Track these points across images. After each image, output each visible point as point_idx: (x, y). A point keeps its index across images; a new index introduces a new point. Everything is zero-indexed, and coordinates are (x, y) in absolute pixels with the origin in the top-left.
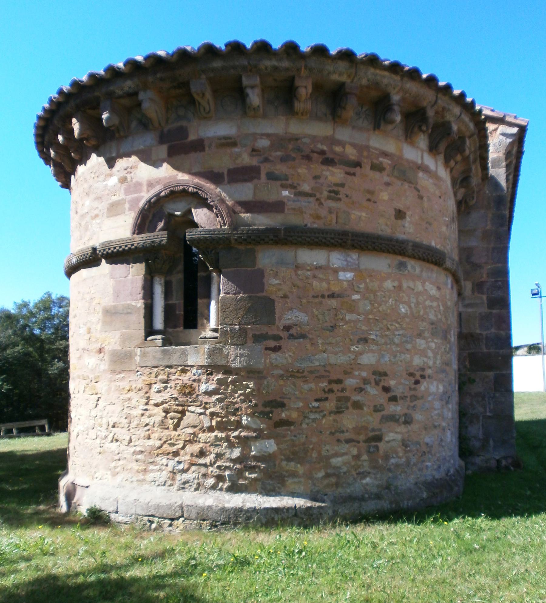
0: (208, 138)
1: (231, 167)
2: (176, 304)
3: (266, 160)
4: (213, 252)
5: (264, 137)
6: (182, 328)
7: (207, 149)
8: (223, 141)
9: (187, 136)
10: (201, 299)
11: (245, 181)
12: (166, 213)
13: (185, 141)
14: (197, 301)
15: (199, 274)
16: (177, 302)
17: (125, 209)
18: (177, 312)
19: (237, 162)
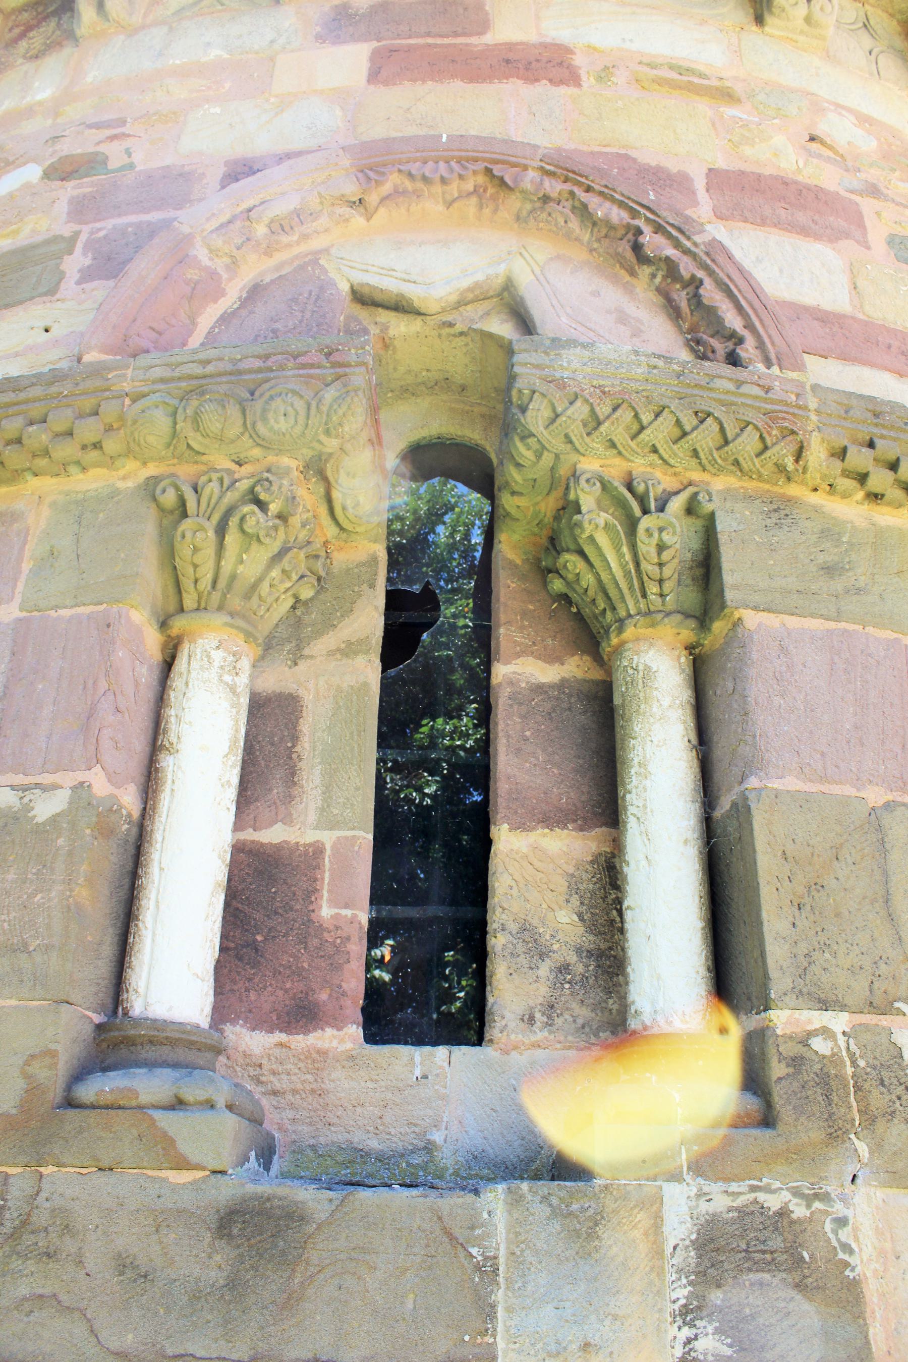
0: (591, 49)
1: (721, 163)
2: (318, 850)
3: (873, 191)
4: (676, 505)
5: (852, 118)
6: (355, 1031)
7: (588, 81)
8: (673, 75)
9: (484, 26)
10: (519, 826)
11: (804, 231)
12: (345, 287)
13: (473, 40)
14: (486, 843)
15: (501, 672)
16: (328, 838)
17: (62, 276)
18: (326, 911)
19: (748, 151)
